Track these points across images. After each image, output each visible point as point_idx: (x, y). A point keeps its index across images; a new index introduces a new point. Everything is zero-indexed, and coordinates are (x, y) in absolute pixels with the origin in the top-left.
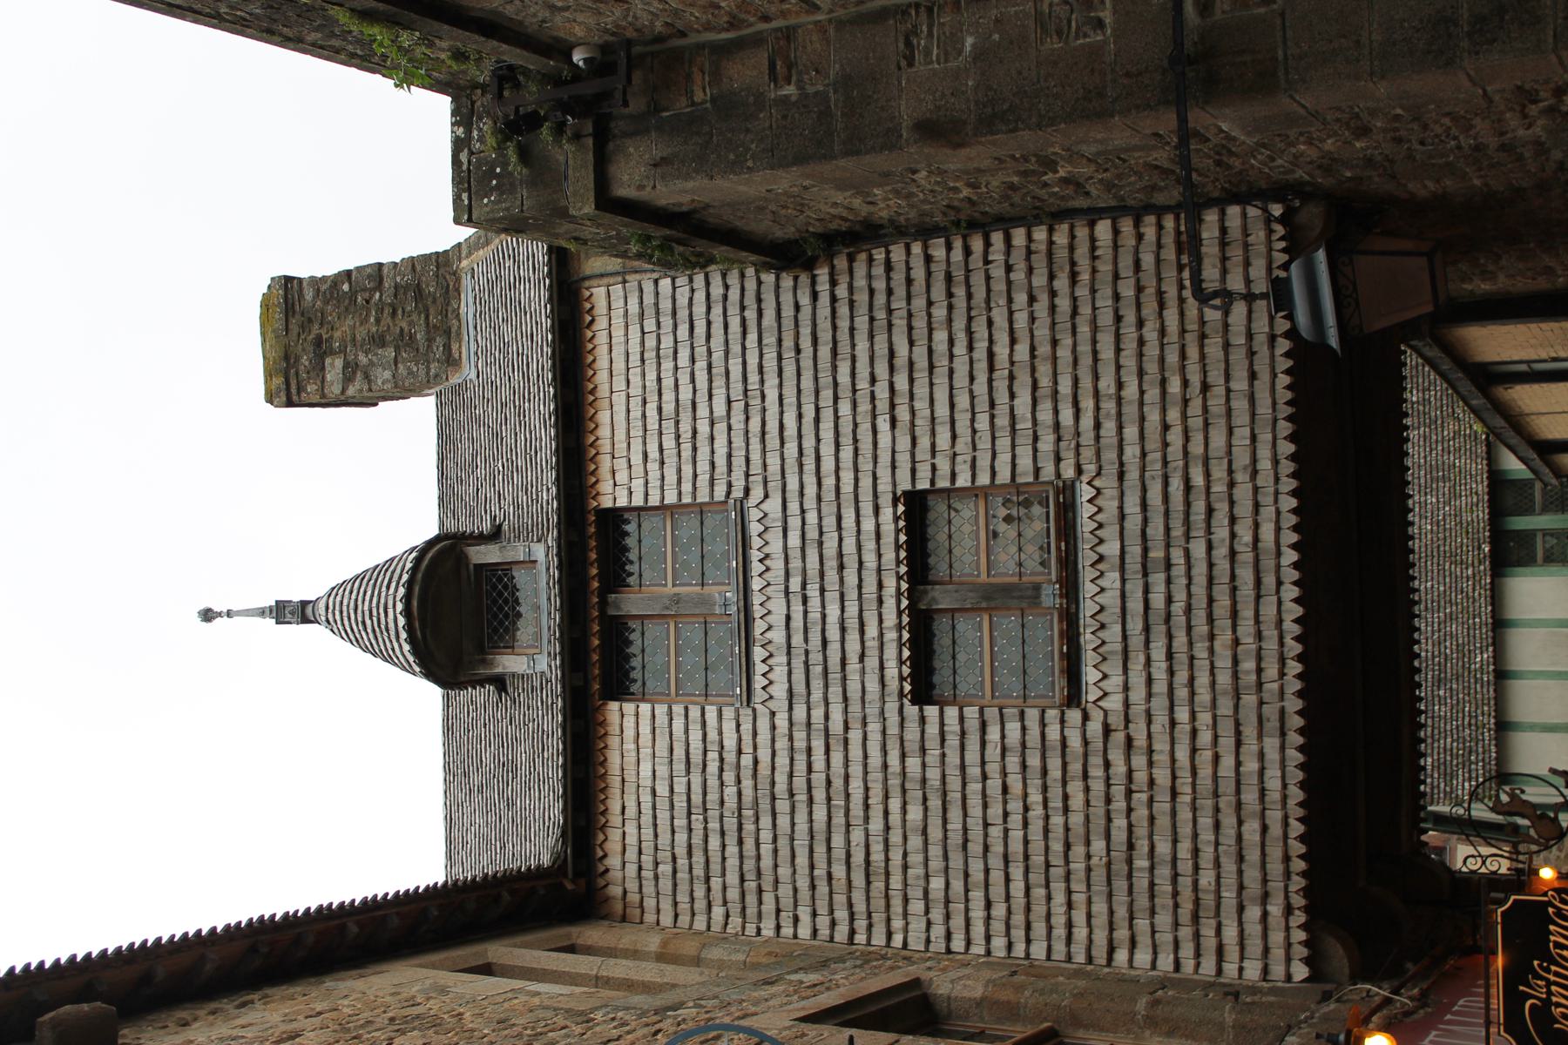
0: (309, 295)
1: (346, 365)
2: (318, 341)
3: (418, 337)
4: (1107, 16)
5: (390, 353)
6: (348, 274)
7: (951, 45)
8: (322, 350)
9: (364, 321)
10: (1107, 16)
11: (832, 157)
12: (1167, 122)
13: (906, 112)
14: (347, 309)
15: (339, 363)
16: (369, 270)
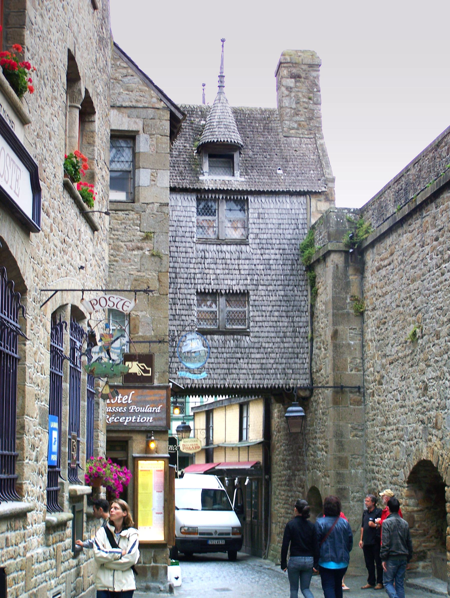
0: (314, 74)
1: (291, 88)
2: (299, 77)
3: (298, 117)
4: (353, 372)
5: (294, 106)
6: (319, 91)
7: (352, 339)
8: (296, 77)
9: (304, 96)
10: (353, 372)
11: (333, 309)
12: (331, 384)
13: (340, 328)
14: (309, 89)
15: (292, 85)
16: (319, 100)
